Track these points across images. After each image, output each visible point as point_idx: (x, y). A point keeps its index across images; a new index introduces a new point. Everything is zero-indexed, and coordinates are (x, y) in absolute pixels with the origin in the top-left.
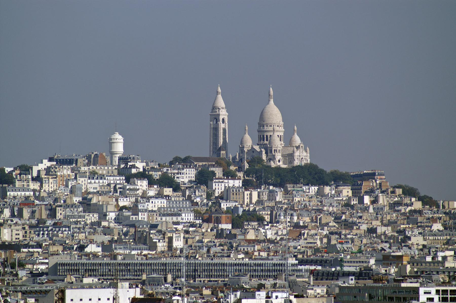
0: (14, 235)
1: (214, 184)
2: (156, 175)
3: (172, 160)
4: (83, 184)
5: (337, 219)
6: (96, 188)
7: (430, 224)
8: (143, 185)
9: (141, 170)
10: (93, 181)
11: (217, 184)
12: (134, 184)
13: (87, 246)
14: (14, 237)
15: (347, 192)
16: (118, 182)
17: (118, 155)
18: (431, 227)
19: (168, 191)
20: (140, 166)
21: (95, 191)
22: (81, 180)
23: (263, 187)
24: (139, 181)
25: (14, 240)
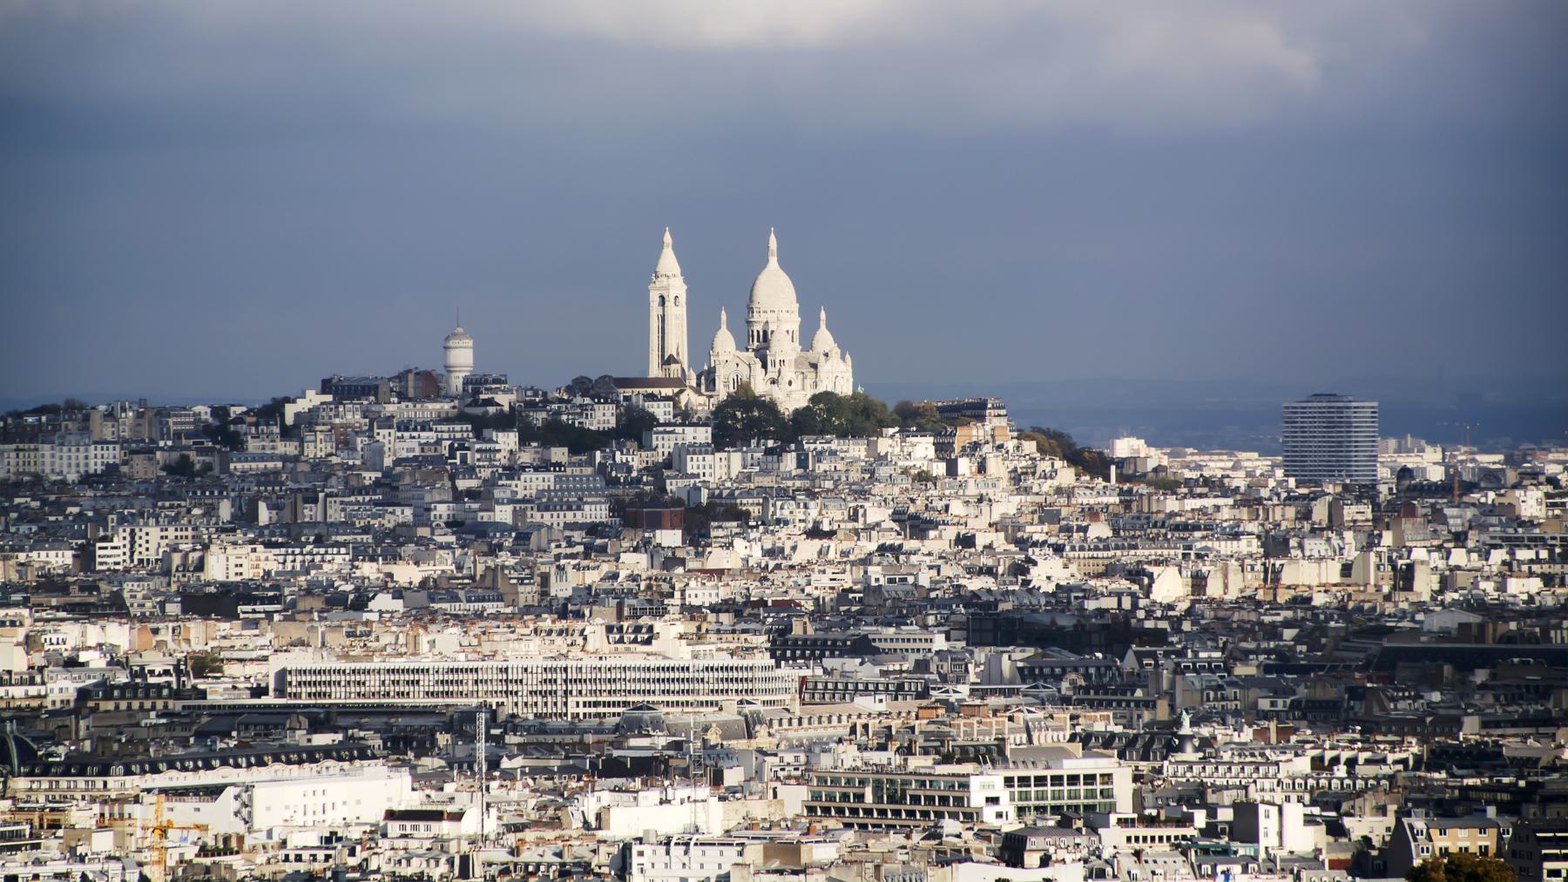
0: (232, 566)
1: (654, 436)
2: (539, 418)
3: (570, 383)
4: (386, 441)
5: (898, 516)
6: (413, 450)
7: (1084, 524)
8: (507, 441)
9: (506, 408)
10: (407, 434)
11: (660, 436)
12: (491, 441)
13: (373, 598)
14: (233, 570)
15: (923, 448)
16: (458, 435)
17: (462, 375)
18: (1085, 530)
19: (559, 454)
20: (504, 400)
21: (411, 455)
22: (384, 436)
23: (754, 442)
24: (500, 434)
25: (233, 578)
